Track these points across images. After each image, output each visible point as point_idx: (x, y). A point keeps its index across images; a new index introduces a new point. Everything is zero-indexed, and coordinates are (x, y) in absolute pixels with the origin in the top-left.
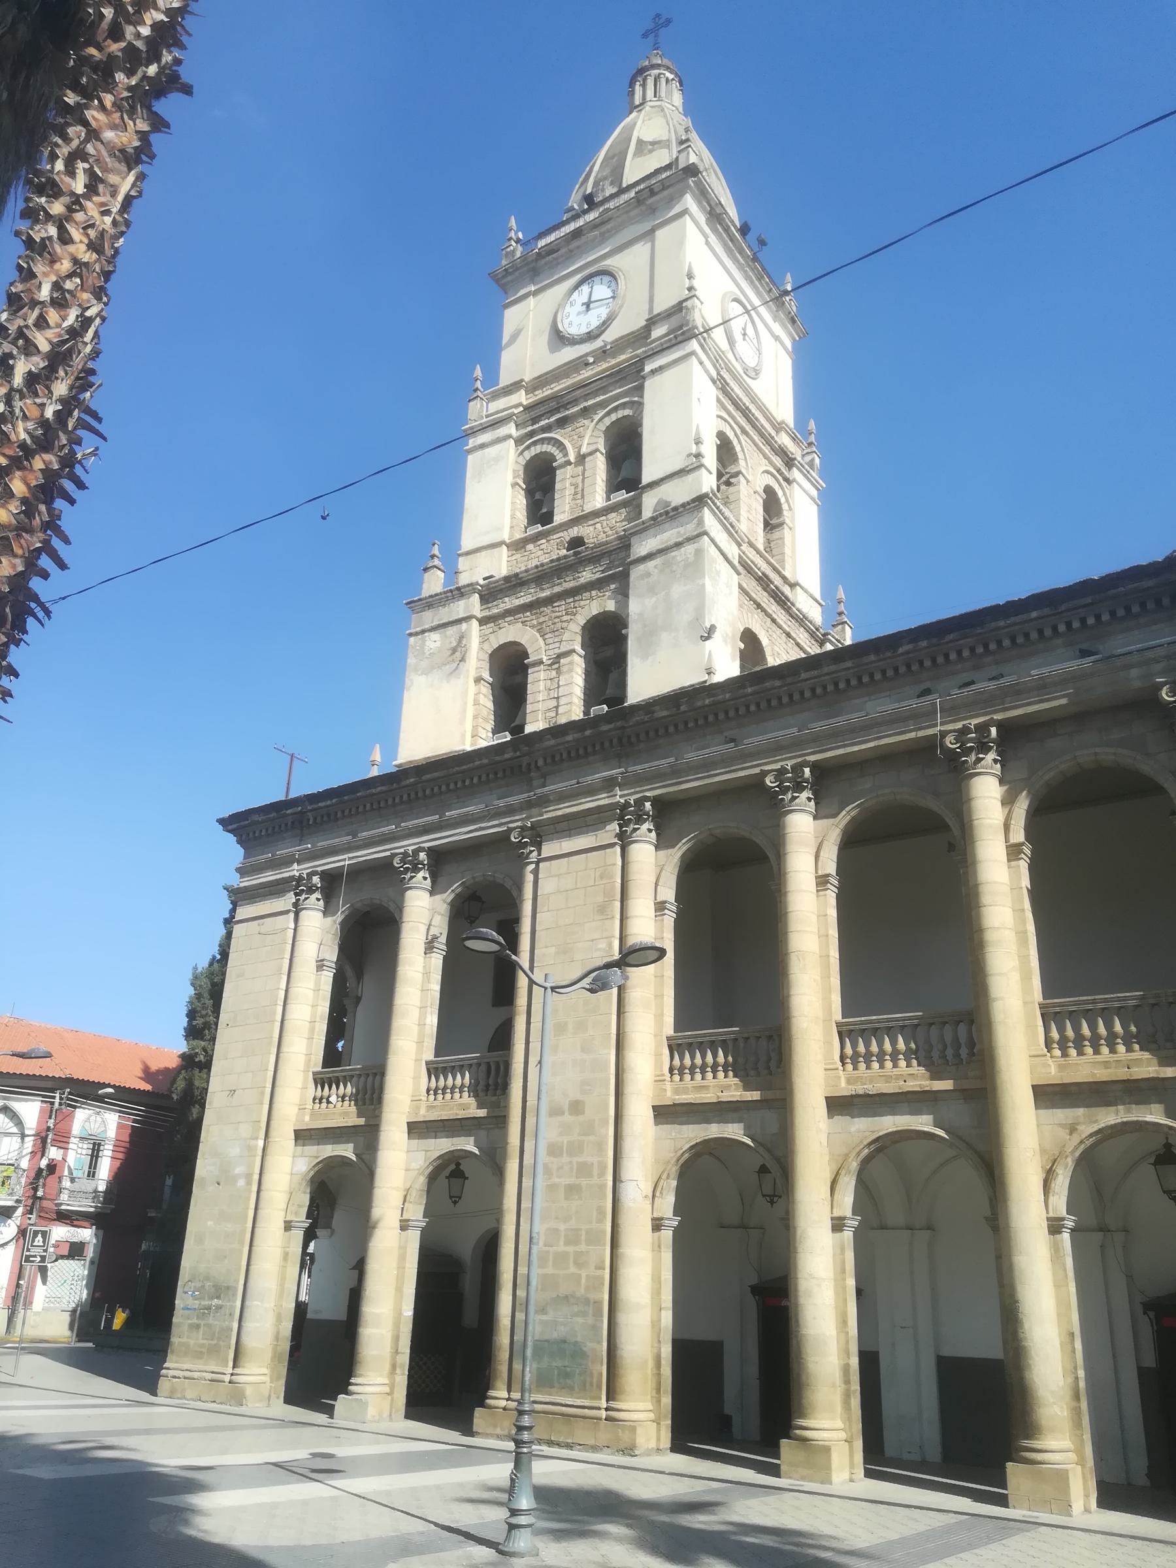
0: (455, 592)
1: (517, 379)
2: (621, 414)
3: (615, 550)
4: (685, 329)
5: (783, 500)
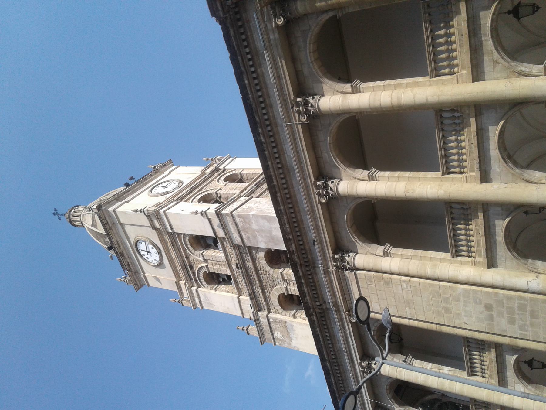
0: (257, 322)
1: (175, 284)
2: (188, 243)
4: (155, 215)
5: (231, 173)
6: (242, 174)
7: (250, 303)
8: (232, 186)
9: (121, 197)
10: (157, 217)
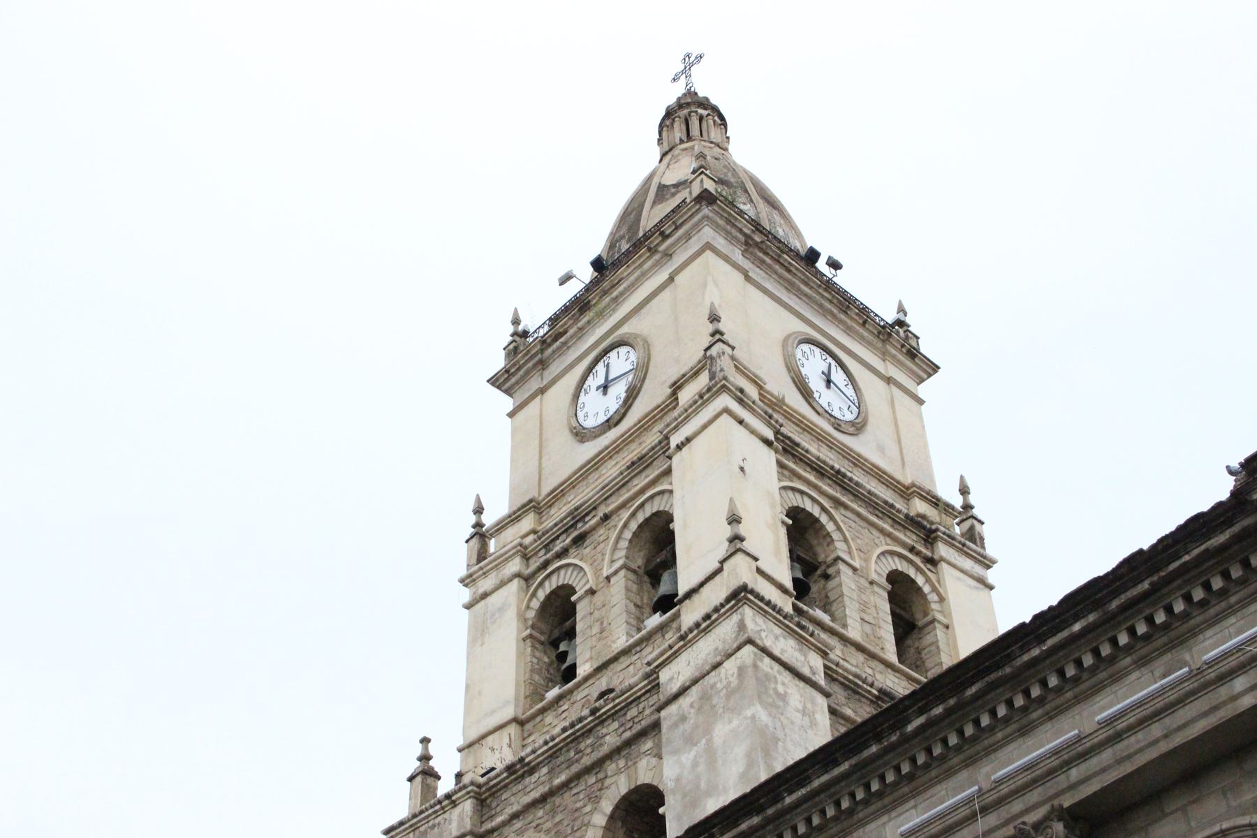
0: (446, 802)
5: (926, 589)
6: (931, 626)
7: (500, 767)
9: (761, 255)
10: (704, 390)
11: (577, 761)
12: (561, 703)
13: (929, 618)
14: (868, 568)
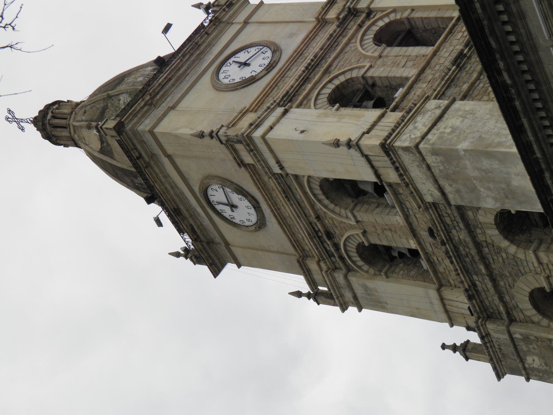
0: (486, 339)
1: (297, 265)
3: (438, 212)
5: (387, 20)
8: (396, 56)
9: (158, 97)
11: (473, 257)
12: (432, 260)
13: (406, 22)
14: (370, 57)
